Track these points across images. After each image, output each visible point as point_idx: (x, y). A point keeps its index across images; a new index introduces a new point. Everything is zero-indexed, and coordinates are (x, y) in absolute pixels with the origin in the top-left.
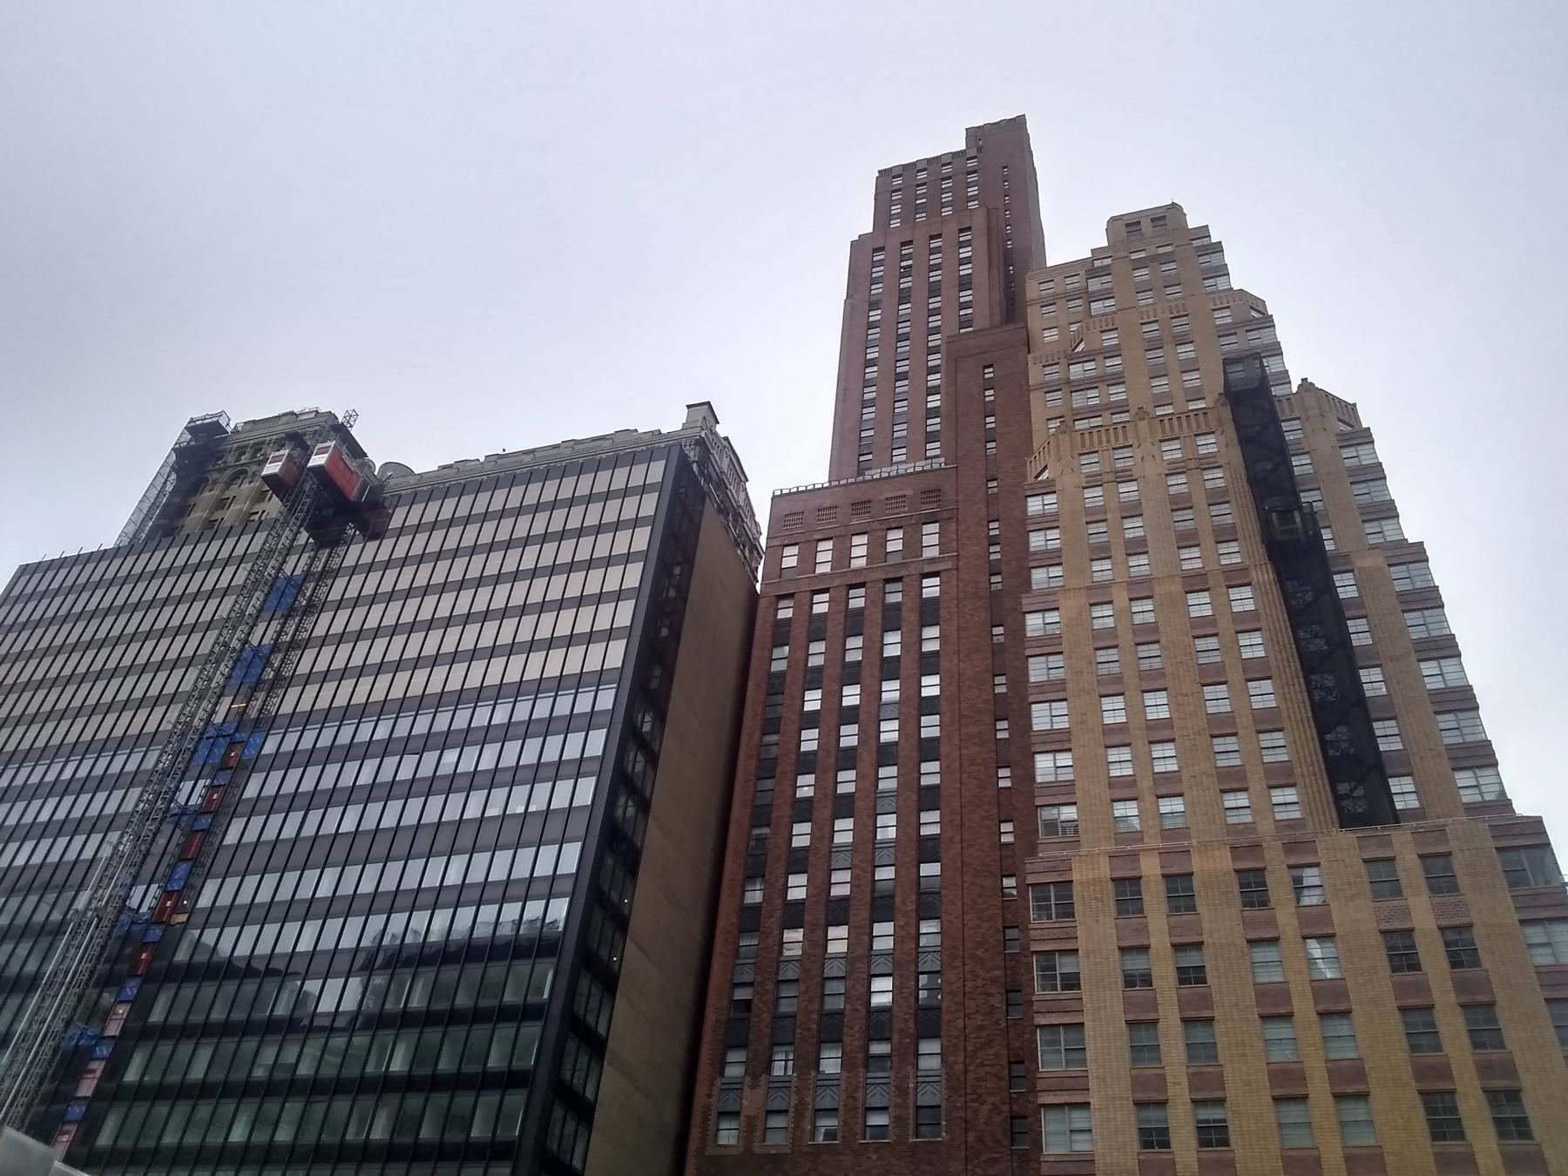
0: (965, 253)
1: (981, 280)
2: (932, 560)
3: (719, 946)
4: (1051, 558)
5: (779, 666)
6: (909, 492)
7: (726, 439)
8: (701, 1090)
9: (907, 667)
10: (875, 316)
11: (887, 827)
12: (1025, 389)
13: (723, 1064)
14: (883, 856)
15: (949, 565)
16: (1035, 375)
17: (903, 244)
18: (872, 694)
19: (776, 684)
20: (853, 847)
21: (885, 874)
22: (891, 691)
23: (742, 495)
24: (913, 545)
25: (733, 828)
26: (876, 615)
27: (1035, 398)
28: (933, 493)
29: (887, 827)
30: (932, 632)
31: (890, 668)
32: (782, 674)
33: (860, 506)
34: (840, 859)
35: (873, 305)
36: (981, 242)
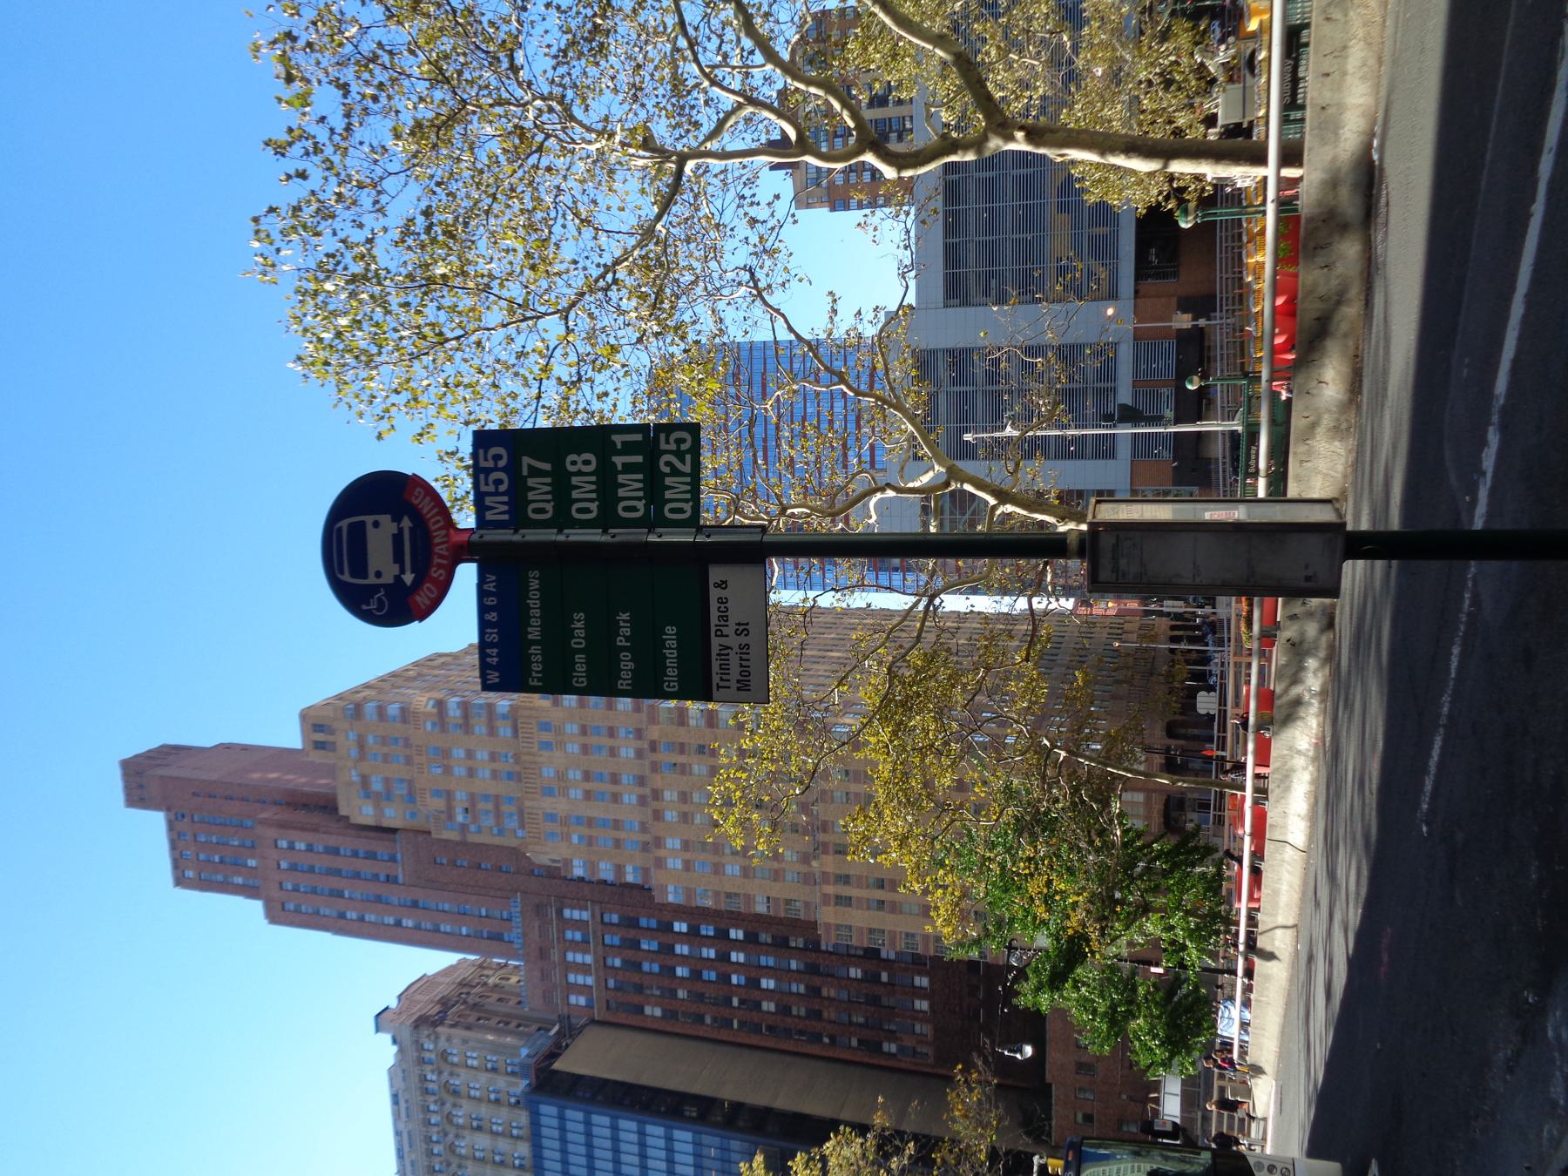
0: (301, 846)
1: (333, 841)
2: (593, 916)
3: (830, 1054)
4: (619, 869)
5: (658, 1012)
6: (537, 924)
7: (400, 997)
8: (903, 1066)
9: (667, 939)
10: (352, 915)
11: (767, 960)
12: (463, 843)
13: (890, 1055)
14: (784, 965)
15: (597, 908)
16: (452, 835)
17: (281, 888)
18: (684, 960)
19: (670, 1015)
20: (778, 980)
21: (794, 965)
22: (682, 949)
23: (440, 979)
24: (579, 925)
25: (762, 1044)
26: (629, 953)
27: (473, 838)
28: (539, 910)
29: (767, 960)
30: (643, 922)
31: (667, 949)
32: (664, 1011)
33: (543, 954)
34: (785, 987)
35: (342, 916)
36: (293, 834)
